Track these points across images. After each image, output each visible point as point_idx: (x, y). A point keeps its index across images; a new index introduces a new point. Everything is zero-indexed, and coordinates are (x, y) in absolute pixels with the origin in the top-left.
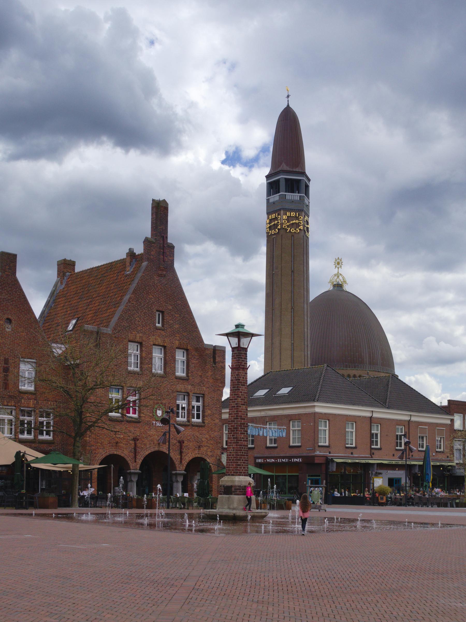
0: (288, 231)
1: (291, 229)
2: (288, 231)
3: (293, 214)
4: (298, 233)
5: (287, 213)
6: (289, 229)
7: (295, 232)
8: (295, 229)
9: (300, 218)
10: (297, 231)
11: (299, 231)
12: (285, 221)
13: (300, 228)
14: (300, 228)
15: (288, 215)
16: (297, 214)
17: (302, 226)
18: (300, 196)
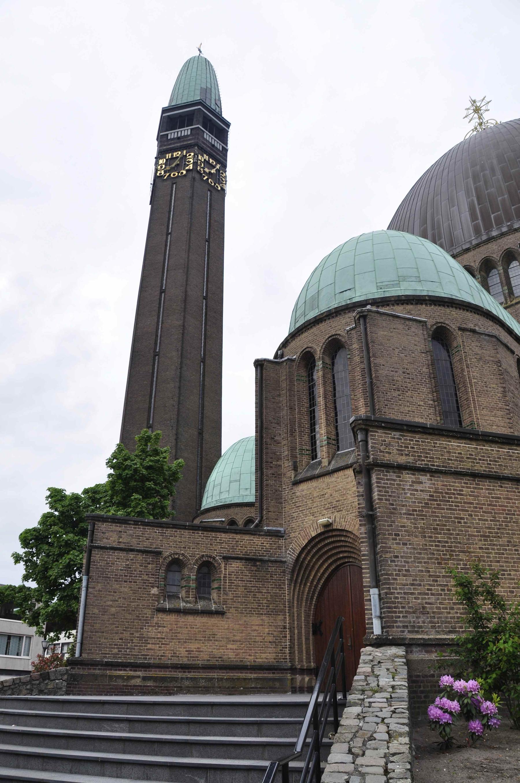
0: (165, 178)
1: (170, 175)
2: (165, 178)
3: (178, 154)
4: (185, 175)
5: (167, 155)
6: (168, 174)
7: (178, 176)
8: (178, 173)
9: (190, 155)
10: (182, 173)
11: (184, 172)
12: (161, 167)
13: (187, 168)
14: (187, 168)
15: (167, 158)
16: (185, 152)
17: (191, 165)
18: (191, 129)
